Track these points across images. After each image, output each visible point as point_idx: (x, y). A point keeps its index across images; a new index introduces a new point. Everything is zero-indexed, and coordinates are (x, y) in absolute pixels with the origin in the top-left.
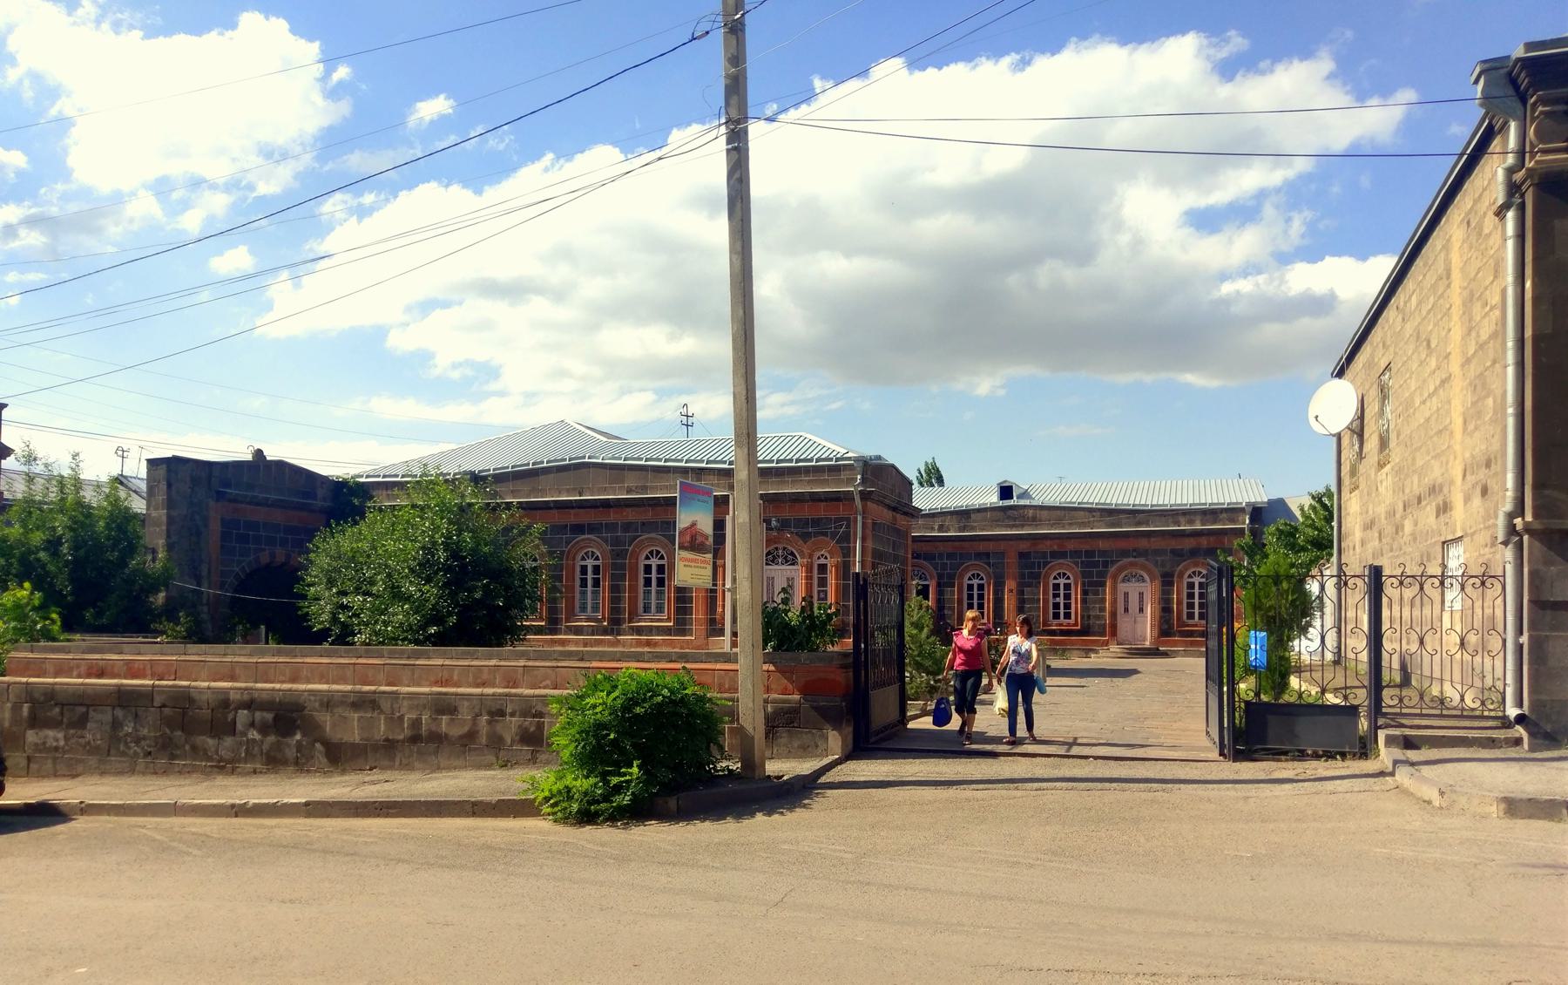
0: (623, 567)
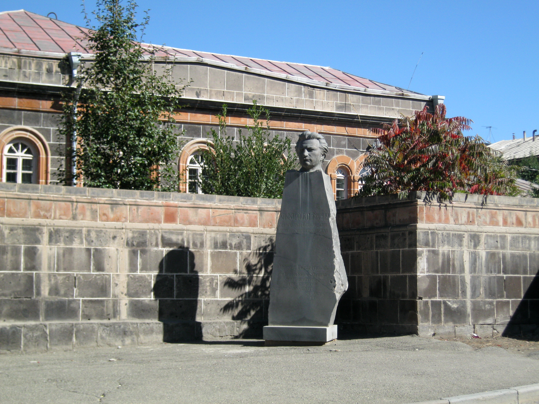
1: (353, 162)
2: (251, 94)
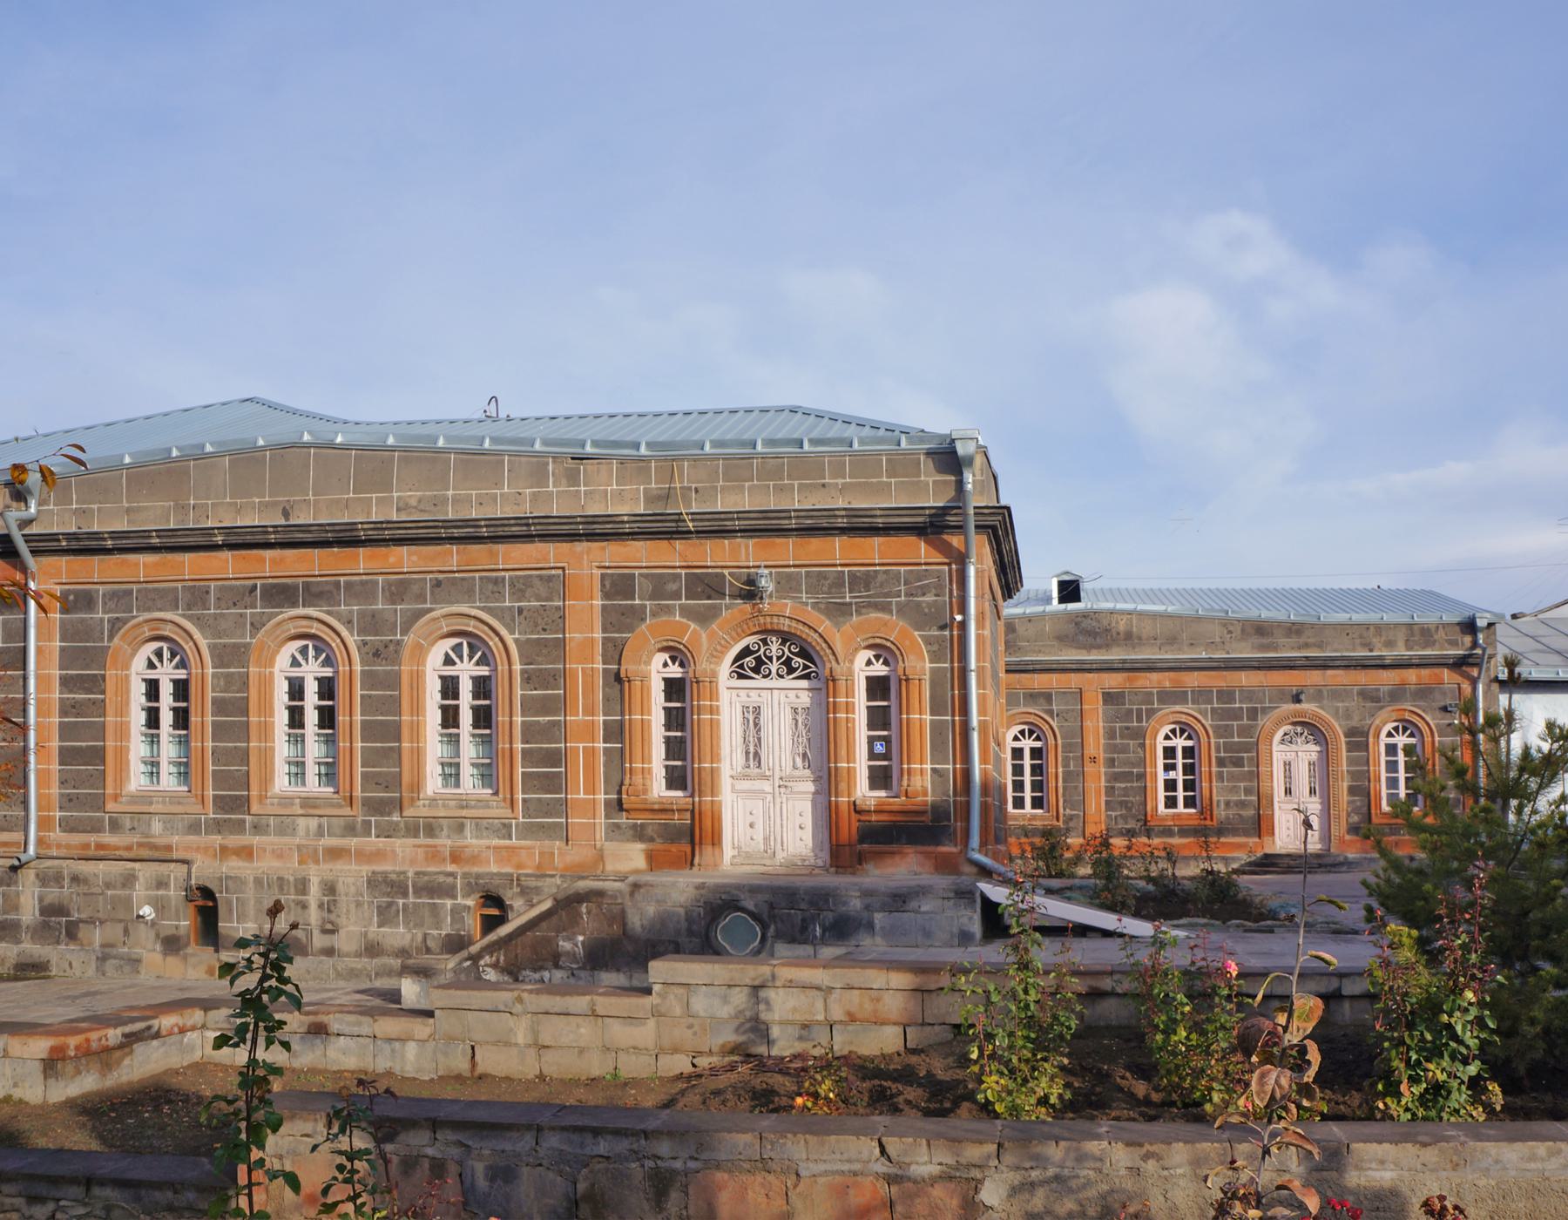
0: (393, 681)
2: (412, 496)
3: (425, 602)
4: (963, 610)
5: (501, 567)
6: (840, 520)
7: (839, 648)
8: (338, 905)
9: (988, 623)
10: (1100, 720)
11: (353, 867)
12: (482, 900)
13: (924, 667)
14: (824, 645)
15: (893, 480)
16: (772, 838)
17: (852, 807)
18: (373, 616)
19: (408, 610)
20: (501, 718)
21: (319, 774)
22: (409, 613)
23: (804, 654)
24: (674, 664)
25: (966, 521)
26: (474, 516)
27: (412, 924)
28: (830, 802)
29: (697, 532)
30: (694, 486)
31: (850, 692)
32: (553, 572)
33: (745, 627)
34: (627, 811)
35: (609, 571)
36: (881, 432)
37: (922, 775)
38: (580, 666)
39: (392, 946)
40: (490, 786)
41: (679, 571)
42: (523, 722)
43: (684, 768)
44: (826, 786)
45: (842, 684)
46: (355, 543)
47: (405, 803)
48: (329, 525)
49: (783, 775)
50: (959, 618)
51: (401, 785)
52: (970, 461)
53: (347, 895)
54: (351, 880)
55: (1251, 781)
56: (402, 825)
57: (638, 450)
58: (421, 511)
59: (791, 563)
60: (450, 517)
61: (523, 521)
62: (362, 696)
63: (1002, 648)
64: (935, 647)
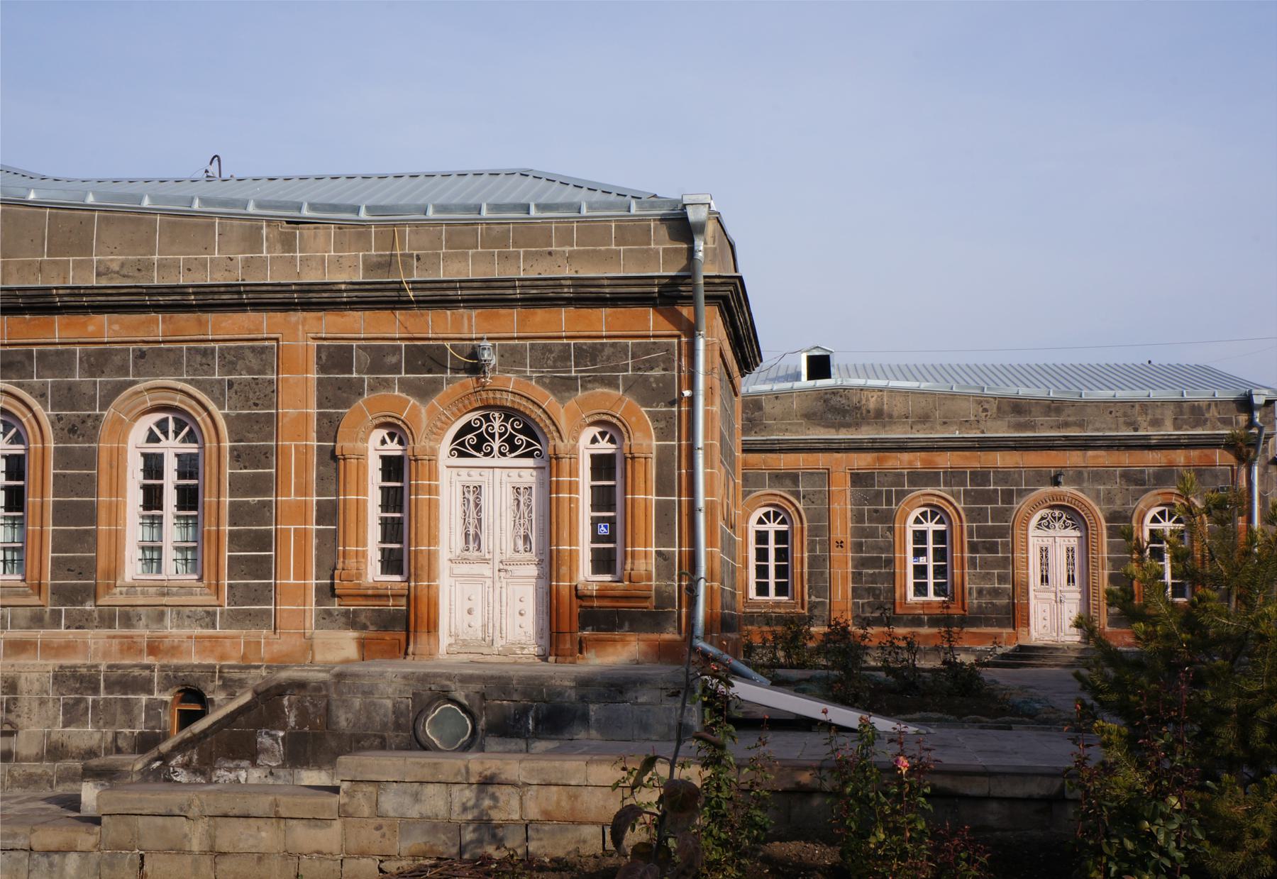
0: (89, 459)
1: (415, 412)
2: (114, 260)
3: (127, 374)
4: (692, 385)
5: (210, 337)
6: (566, 290)
7: (563, 424)
8: (19, 704)
9: (717, 400)
10: (848, 501)
11: (39, 661)
12: (180, 695)
13: (650, 446)
14: (548, 422)
15: (622, 248)
16: (491, 625)
17: (574, 592)
18: (70, 389)
19: (107, 382)
20: (207, 498)
21: (5, 561)
22: (109, 387)
23: (528, 431)
24: (392, 440)
25: (695, 291)
26: (181, 283)
27: (101, 723)
28: (551, 586)
29: (418, 302)
30: (415, 253)
31: (573, 472)
32: (266, 343)
33: (466, 402)
34: (339, 596)
35: (325, 343)
36: (613, 197)
37: (646, 557)
38: (293, 443)
39: (77, 747)
40: (194, 571)
41: (399, 343)
42: (231, 503)
43: (401, 550)
44: (547, 570)
45: (565, 463)
46: (51, 309)
47: (101, 590)
48: (19, 289)
49: (504, 558)
50: (687, 393)
51: (96, 571)
52: (701, 228)
53: (29, 692)
54: (35, 676)
55: (1005, 567)
56: (96, 615)
57: (358, 214)
58: (124, 276)
59: (515, 335)
60: (156, 283)
61: (234, 289)
62: (55, 476)
63: (738, 425)
64: (662, 424)
